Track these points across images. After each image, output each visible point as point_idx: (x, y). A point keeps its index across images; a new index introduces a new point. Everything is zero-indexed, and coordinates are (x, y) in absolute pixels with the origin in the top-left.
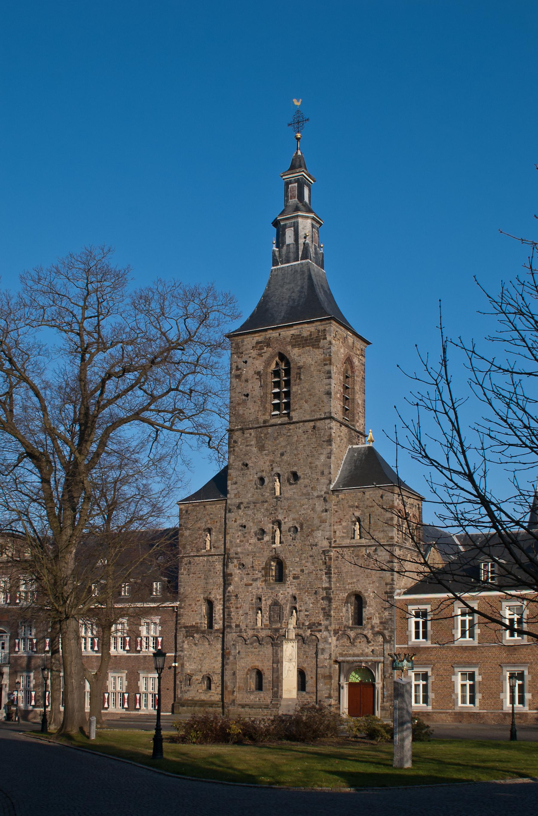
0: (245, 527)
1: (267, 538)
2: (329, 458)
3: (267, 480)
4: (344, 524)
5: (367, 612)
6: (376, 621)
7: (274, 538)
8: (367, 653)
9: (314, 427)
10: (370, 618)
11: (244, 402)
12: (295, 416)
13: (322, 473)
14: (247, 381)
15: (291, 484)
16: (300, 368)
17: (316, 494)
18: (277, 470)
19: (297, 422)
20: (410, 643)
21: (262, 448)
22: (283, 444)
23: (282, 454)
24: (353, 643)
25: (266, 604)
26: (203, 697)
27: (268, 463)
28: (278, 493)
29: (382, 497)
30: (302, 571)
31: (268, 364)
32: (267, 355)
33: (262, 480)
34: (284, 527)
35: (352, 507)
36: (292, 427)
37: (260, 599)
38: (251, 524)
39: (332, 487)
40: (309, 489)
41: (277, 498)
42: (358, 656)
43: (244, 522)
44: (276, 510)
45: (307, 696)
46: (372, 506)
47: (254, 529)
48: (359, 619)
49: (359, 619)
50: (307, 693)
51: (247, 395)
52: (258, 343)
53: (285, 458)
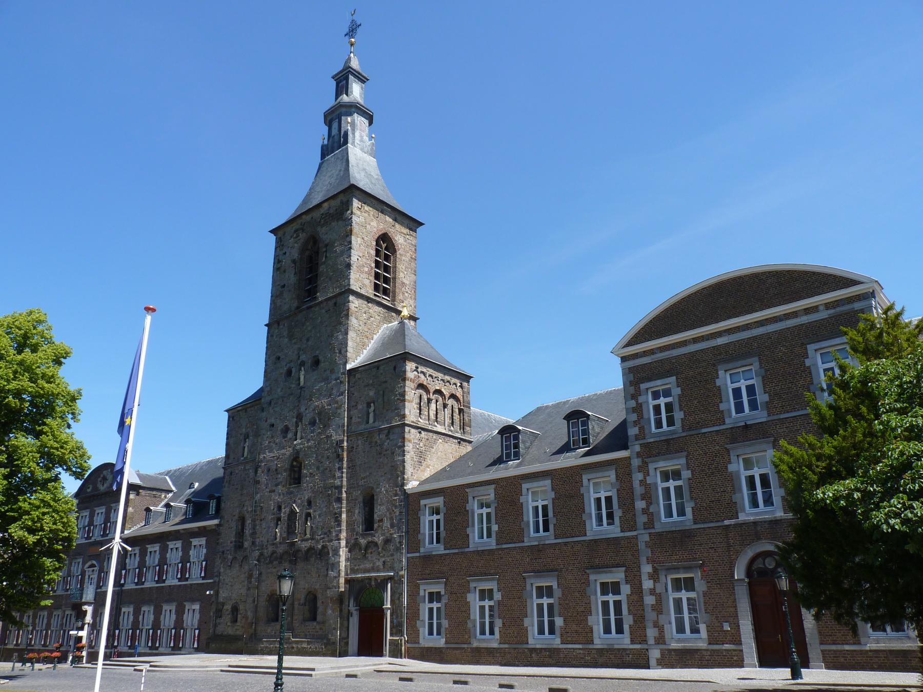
0: (273, 425)
1: (290, 435)
2: (347, 334)
3: (294, 370)
4: (360, 407)
5: (380, 510)
6: (386, 524)
7: (296, 435)
8: (378, 567)
9: (335, 304)
10: (381, 521)
11: (281, 293)
12: (321, 297)
13: (340, 352)
14: (285, 271)
15: (314, 370)
16: (327, 245)
17: (334, 377)
18: (303, 357)
19: (321, 302)
20: (422, 550)
21: (291, 337)
22: (309, 328)
23: (308, 340)
24: (365, 556)
25: (284, 515)
26: (230, 631)
27: (296, 352)
28: (302, 384)
29: (395, 368)
30: (318, 468)
31: (302, 251)
32: (302, 241)
33: (289, 373)
34: (306, 420)
35: (365, 386)
36: (317, 309)
37: (280, 508)
38: (278, 421)
39: (349, 367)
40: (328, 372)
41: (301, 388)
42: (368, 571)
43: (272, 421)
44: (299, 401)
45: (318, 627)
46: (386, 382)
47: (280, 427)
48: (369, 524)
49: (369, 524)
50: (319, 623)
51: (284, 286)
52: (295, 231)
53: (310, 343)
